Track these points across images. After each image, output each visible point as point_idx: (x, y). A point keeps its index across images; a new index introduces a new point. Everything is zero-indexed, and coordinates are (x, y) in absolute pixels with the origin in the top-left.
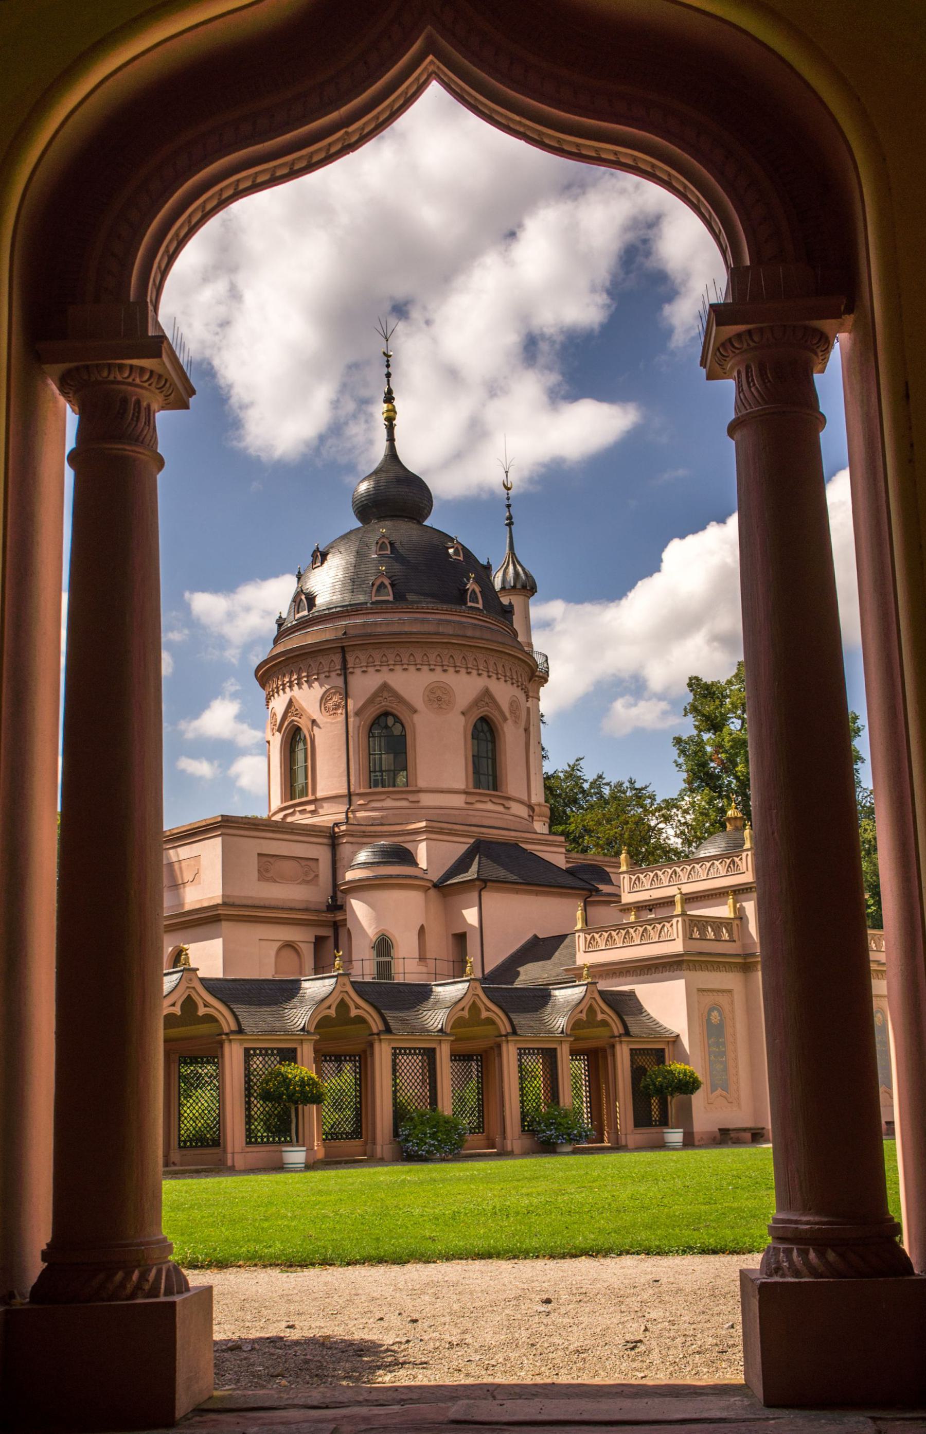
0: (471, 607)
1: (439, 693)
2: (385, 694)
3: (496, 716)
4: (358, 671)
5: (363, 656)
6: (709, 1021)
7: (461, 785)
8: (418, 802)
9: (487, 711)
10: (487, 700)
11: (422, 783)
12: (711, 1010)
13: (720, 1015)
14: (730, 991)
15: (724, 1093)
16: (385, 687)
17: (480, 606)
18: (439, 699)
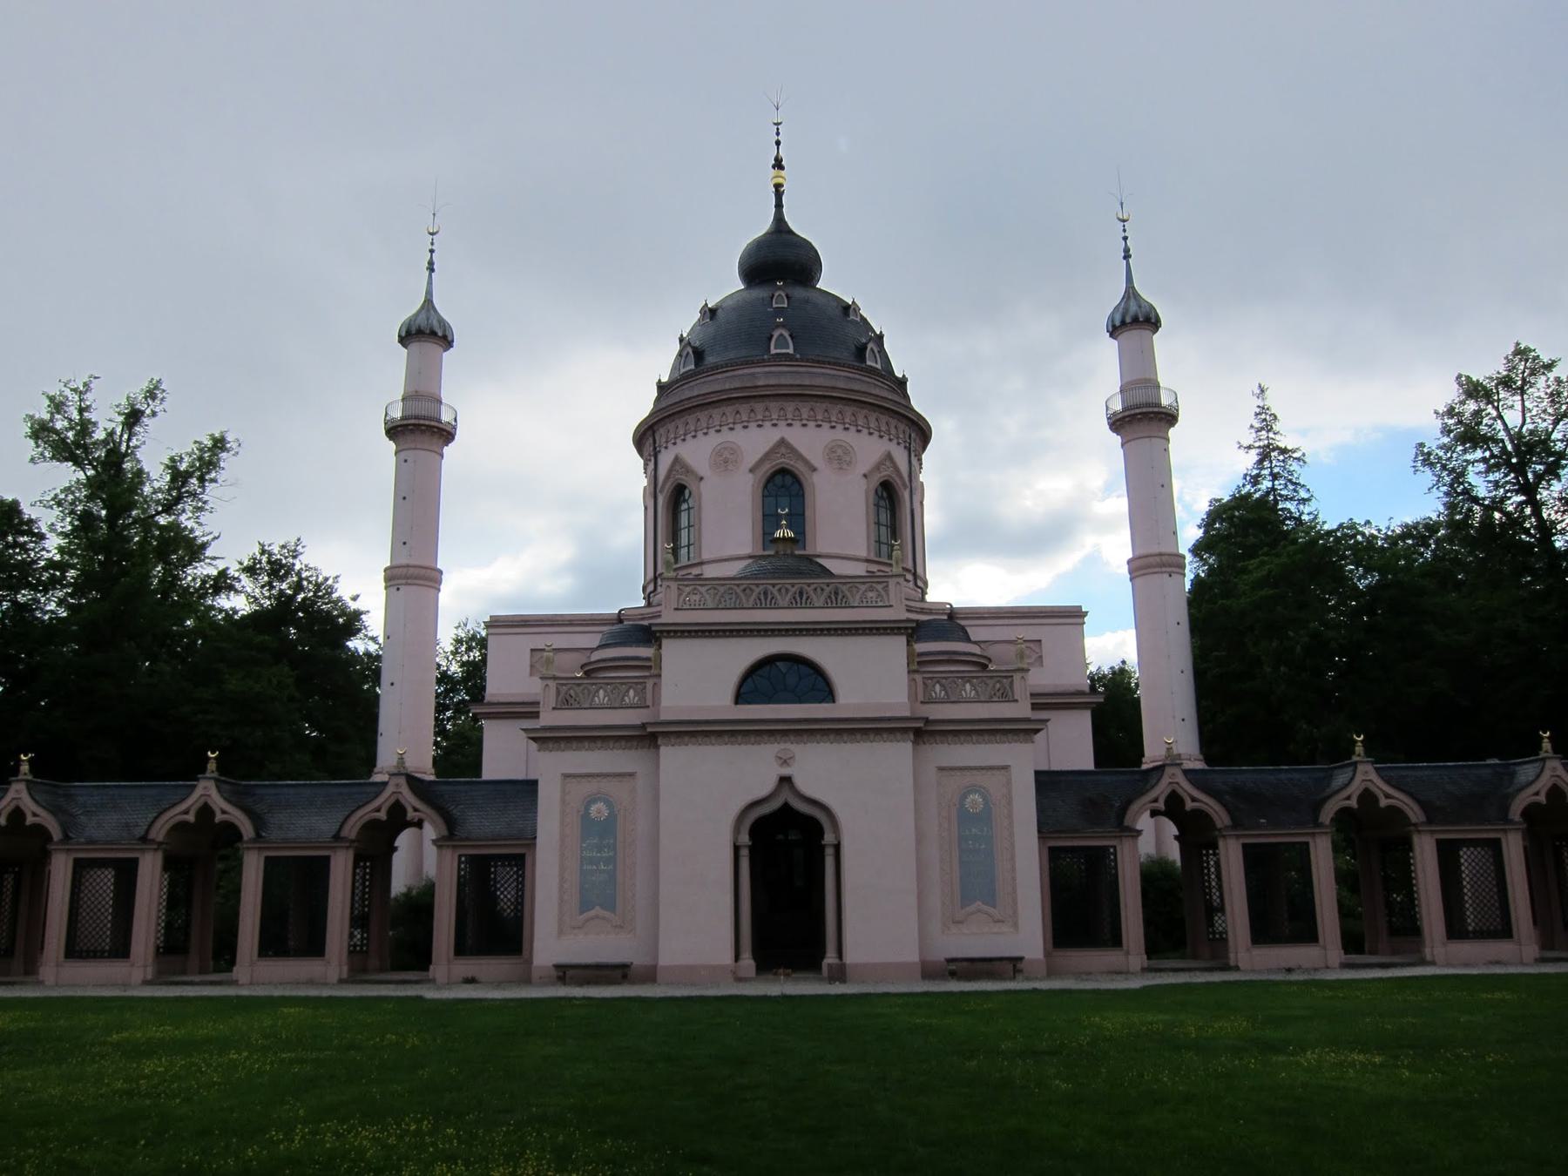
0: (777, 354)
1: (726, 454)
2: (677, 467)
3: (799, 468)
4: (663, 450)
5: (662, 431)
6: (586, 816)
7: (748, 550)
8: (702, 575)
9: (781, 463)
10: (783, 450)
11: (706, 556)
12: (590, 801)
13: (609, 804)
14: (631, 775)
15: (607, 914)
16: (677, 460)
17: (791, 351)
18: (726, 461)
